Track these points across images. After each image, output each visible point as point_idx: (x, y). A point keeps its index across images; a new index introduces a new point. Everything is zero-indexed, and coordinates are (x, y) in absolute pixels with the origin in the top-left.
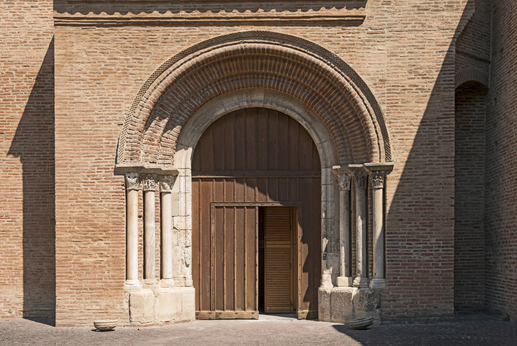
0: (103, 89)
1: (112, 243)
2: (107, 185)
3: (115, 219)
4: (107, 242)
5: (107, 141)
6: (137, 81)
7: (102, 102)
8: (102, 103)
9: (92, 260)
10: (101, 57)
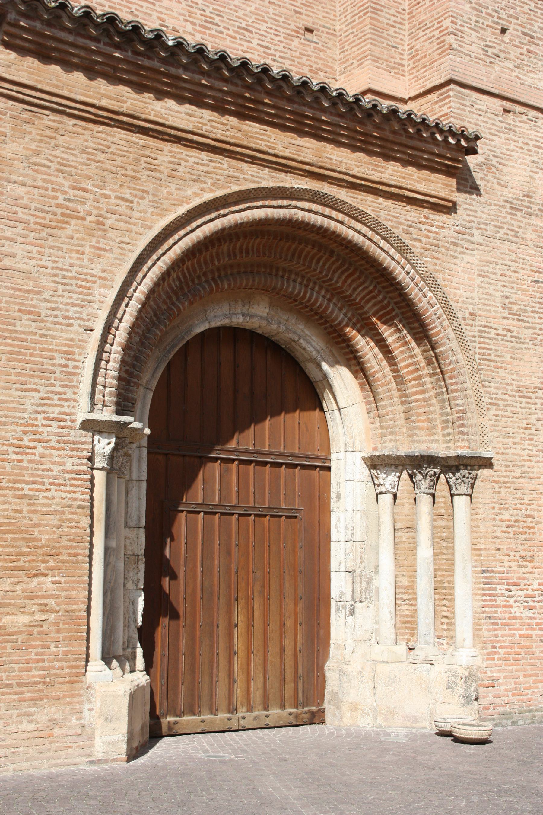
0: (60, 249)
1: (67, 583)
2: (59, 456)
3: (73, 530)
4: (57, 578)
5: (64, 362)
6: (123, 245)
7: (55, 276)
8: (56, 279)
9: (24, 619)
10: (58, 180)
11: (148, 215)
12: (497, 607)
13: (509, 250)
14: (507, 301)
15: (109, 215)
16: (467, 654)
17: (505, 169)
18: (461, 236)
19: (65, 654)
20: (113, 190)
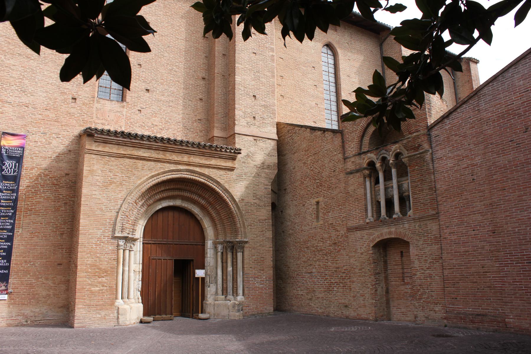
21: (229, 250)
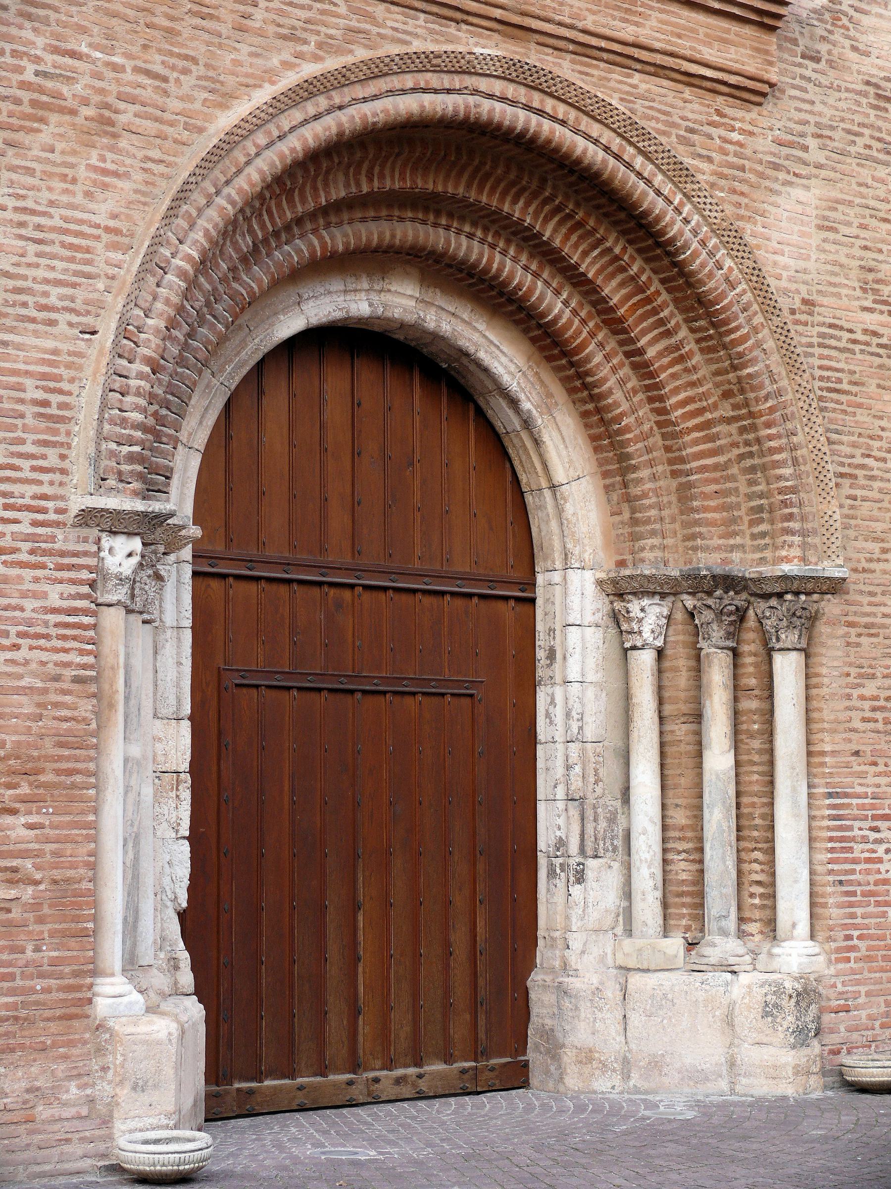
0: (30, 172)
1: (52, 826)
2: (36, 580)
3: (65, 725)
4: (33, 819)
5: (40, 395)
6: (149, 165)
7: (22, 224)
8: (23, 232)
10: (23, 33)
11: (197, 106)
12: (855, 861)
13: (873, 178)
14: (870, 277)
15: (122, 106)
16: (797, 954)
17: (866, 20)
18: (785, 151)
19: (54, 962)
20: (129, 56)
21: (717, 633)
